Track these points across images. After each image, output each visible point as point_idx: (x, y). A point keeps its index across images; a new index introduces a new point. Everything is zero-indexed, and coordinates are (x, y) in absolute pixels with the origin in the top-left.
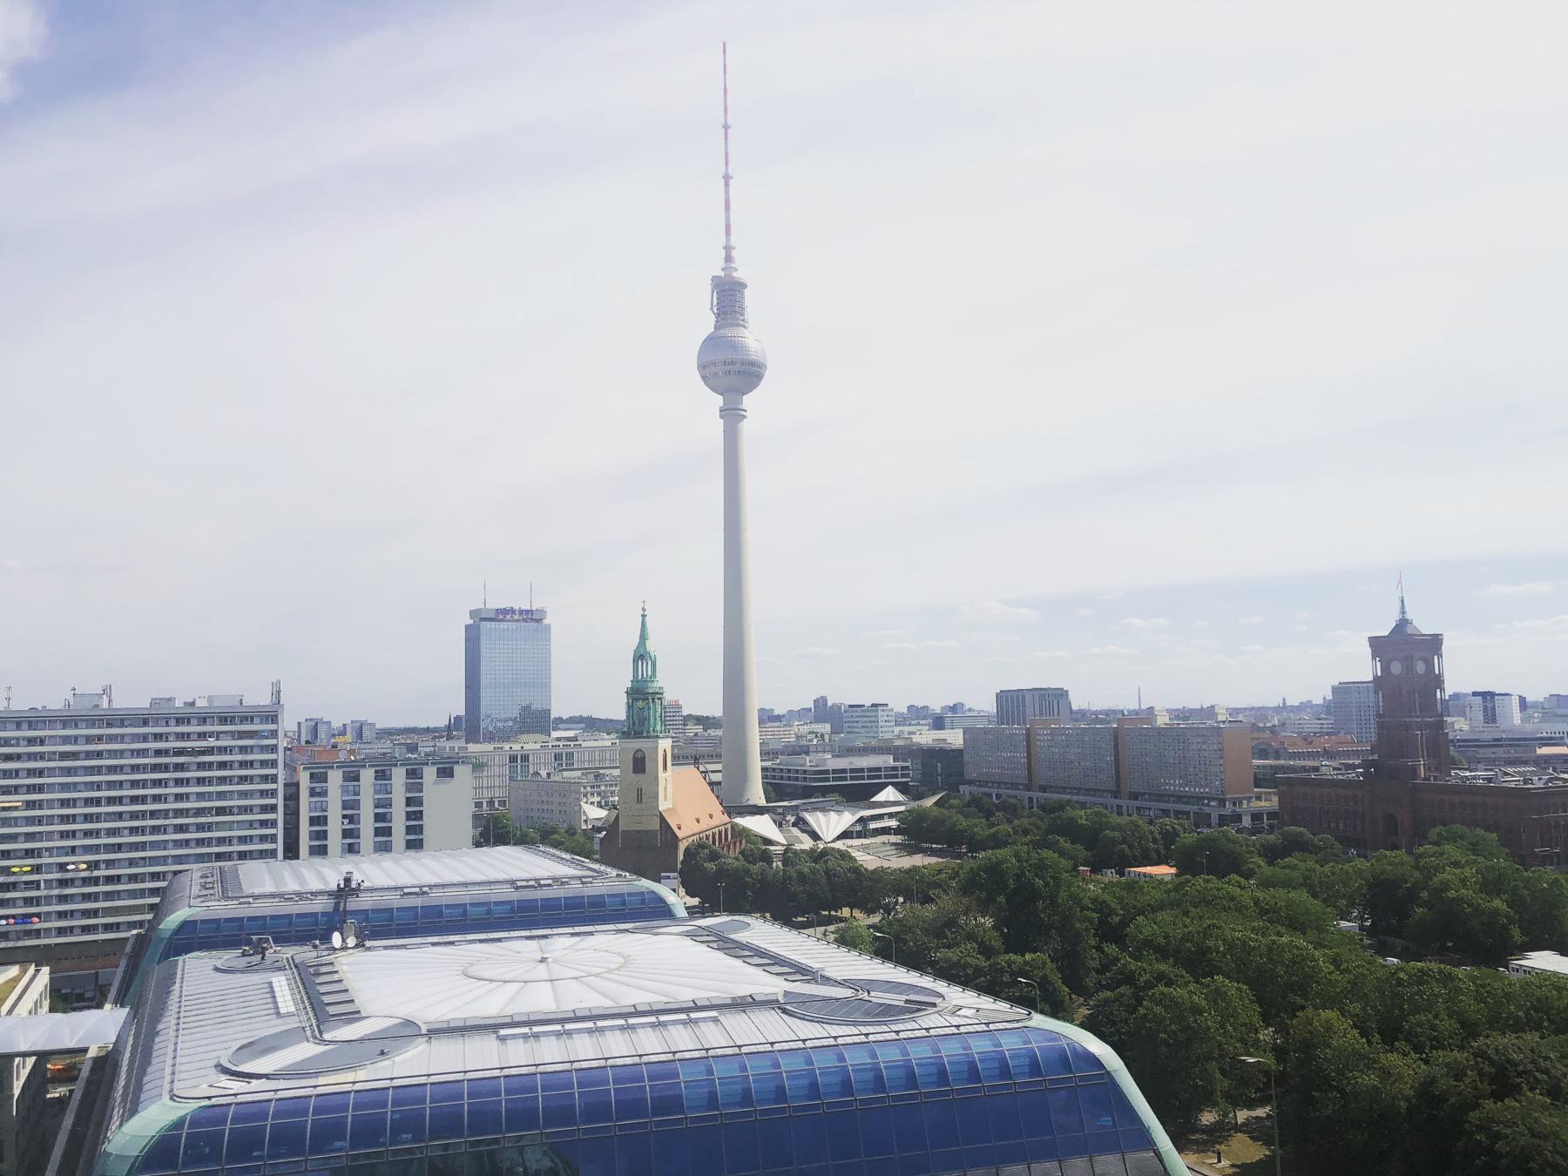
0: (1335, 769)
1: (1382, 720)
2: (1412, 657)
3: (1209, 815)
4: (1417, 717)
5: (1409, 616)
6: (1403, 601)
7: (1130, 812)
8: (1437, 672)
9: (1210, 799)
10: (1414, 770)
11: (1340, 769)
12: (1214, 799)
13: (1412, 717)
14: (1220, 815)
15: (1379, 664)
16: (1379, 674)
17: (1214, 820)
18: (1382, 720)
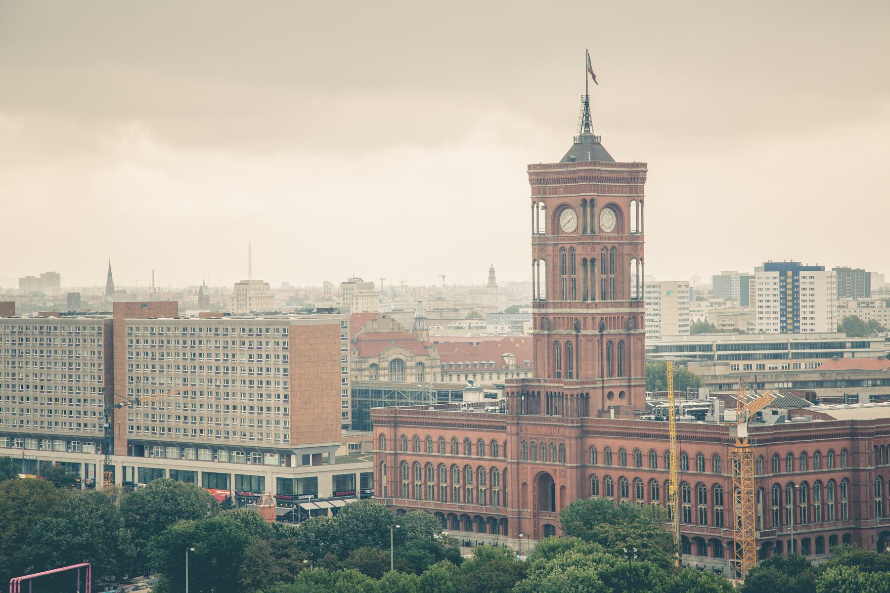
0: (487, 396)
1: (543, 311)
2: (592, 201)
3: (261, 480)
4: (596, 306)
5: (596, 131)
6: (587, 104)
7: (129, 479)
8: (633, 229)
9: (265, 451)
10: (585, 398)
11: (495, 396)
12: (271, 451)
13: (588, 306)
14: (278, 479)
15: (542, 213)
16: (542, 230)
17: (271, 488)
18: (543, 311)
